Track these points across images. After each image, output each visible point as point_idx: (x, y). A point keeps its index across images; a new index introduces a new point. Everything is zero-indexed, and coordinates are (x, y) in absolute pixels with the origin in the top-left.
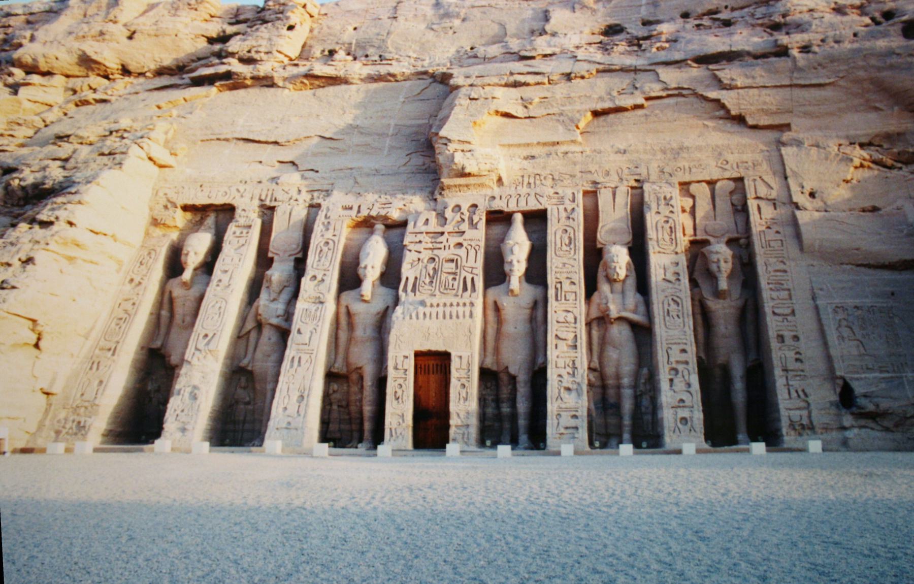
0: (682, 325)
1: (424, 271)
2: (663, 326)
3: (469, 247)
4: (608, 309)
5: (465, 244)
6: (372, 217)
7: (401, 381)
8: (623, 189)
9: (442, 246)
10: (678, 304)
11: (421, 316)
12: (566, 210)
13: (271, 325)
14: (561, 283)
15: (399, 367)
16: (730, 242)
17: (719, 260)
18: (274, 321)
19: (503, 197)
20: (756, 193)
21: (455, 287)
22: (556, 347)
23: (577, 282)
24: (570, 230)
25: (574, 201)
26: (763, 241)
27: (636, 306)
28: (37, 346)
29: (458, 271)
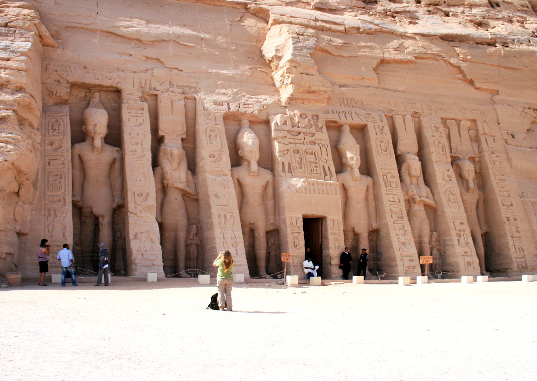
1: (293, 158)
5: (317, 142)
6: (242, 114)
9: (301, 142)
12: (378, 126)
13: (178, 189)
14: (386, 175)
16: (472, 159)
18: (182, 186)
19: (335, 112)
20: (484, 130)
21: (319, 172)
23: (395, 176)
24: (385, 141)
27: (428, 194)
28: (18, 194)
29: (317, 161)
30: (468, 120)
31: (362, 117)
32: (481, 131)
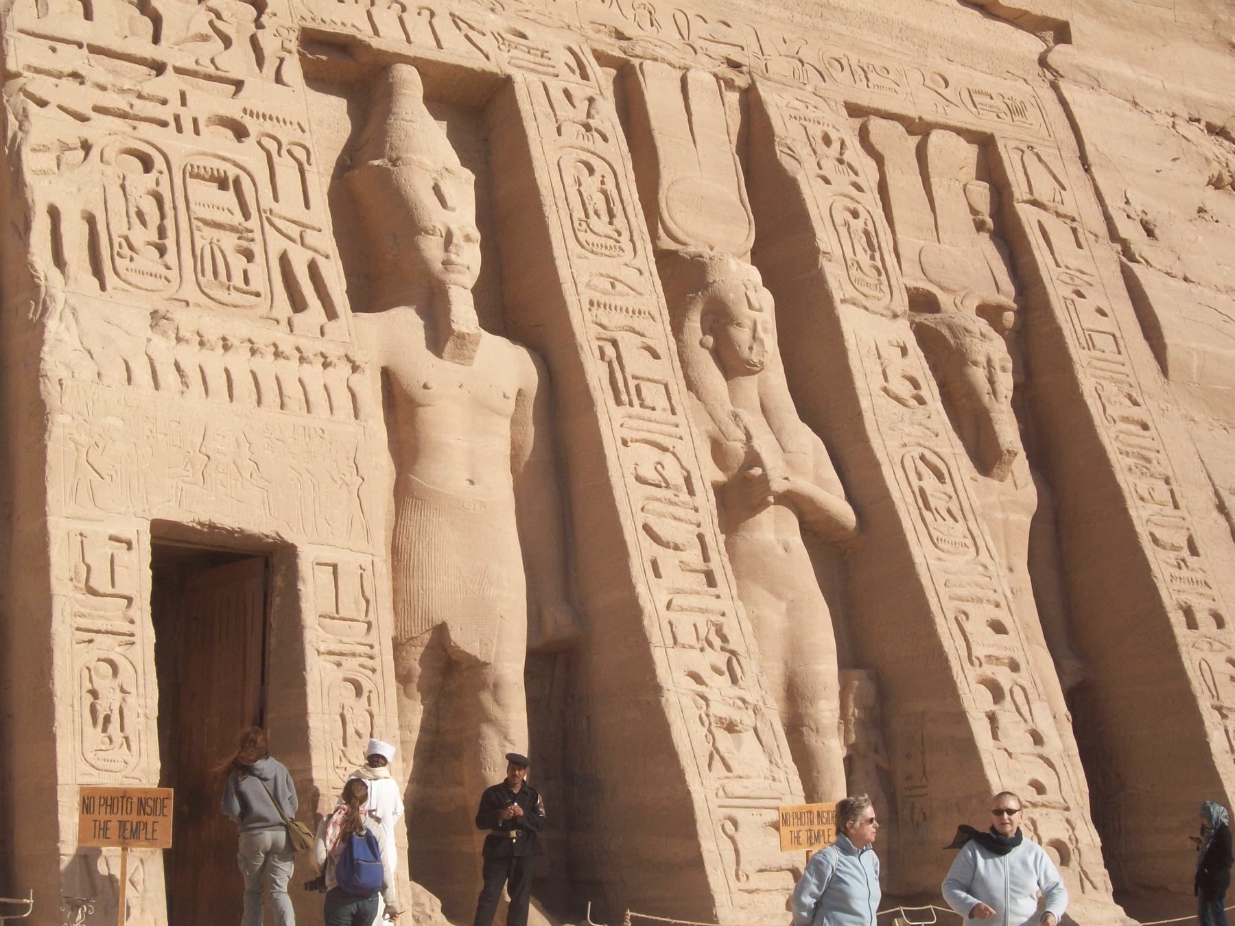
0: (969, 542)
2: (925, 540)
3: (273, 146)
4: (753, 458)
7: (107, 646)
8: (701, 79)
9: (165, 113)
10: (940, 477)
11: (169, 377)
14: (615, 343)
15: (100, 581)
17: (989, 361)
21: (258, 281)
22: (658, 575)
25: (585, 76)
26: (1078, 329)
29: (254, 223)
30: (960, 131)
31: (487, 43)
32: (1019, 190)
